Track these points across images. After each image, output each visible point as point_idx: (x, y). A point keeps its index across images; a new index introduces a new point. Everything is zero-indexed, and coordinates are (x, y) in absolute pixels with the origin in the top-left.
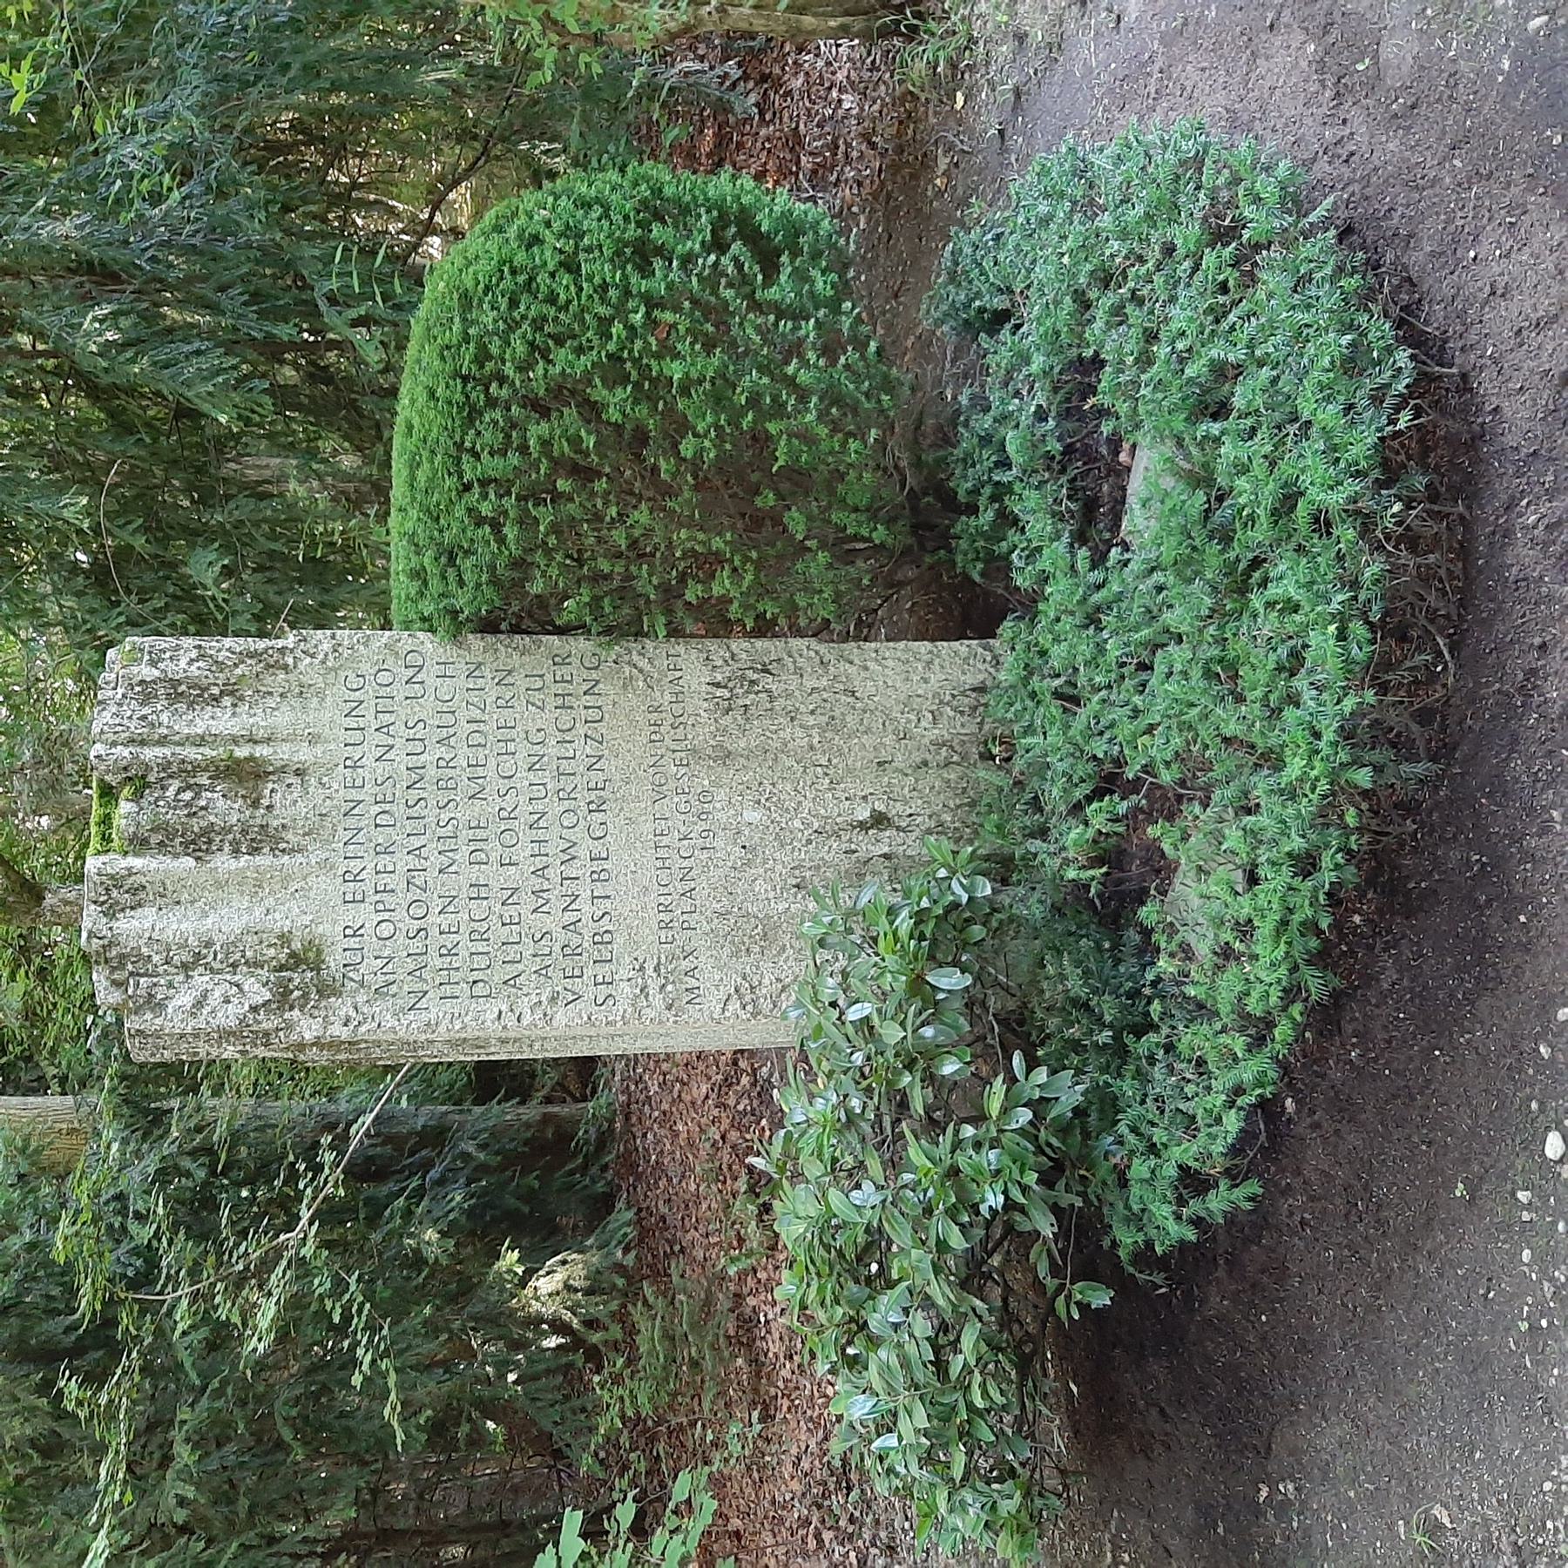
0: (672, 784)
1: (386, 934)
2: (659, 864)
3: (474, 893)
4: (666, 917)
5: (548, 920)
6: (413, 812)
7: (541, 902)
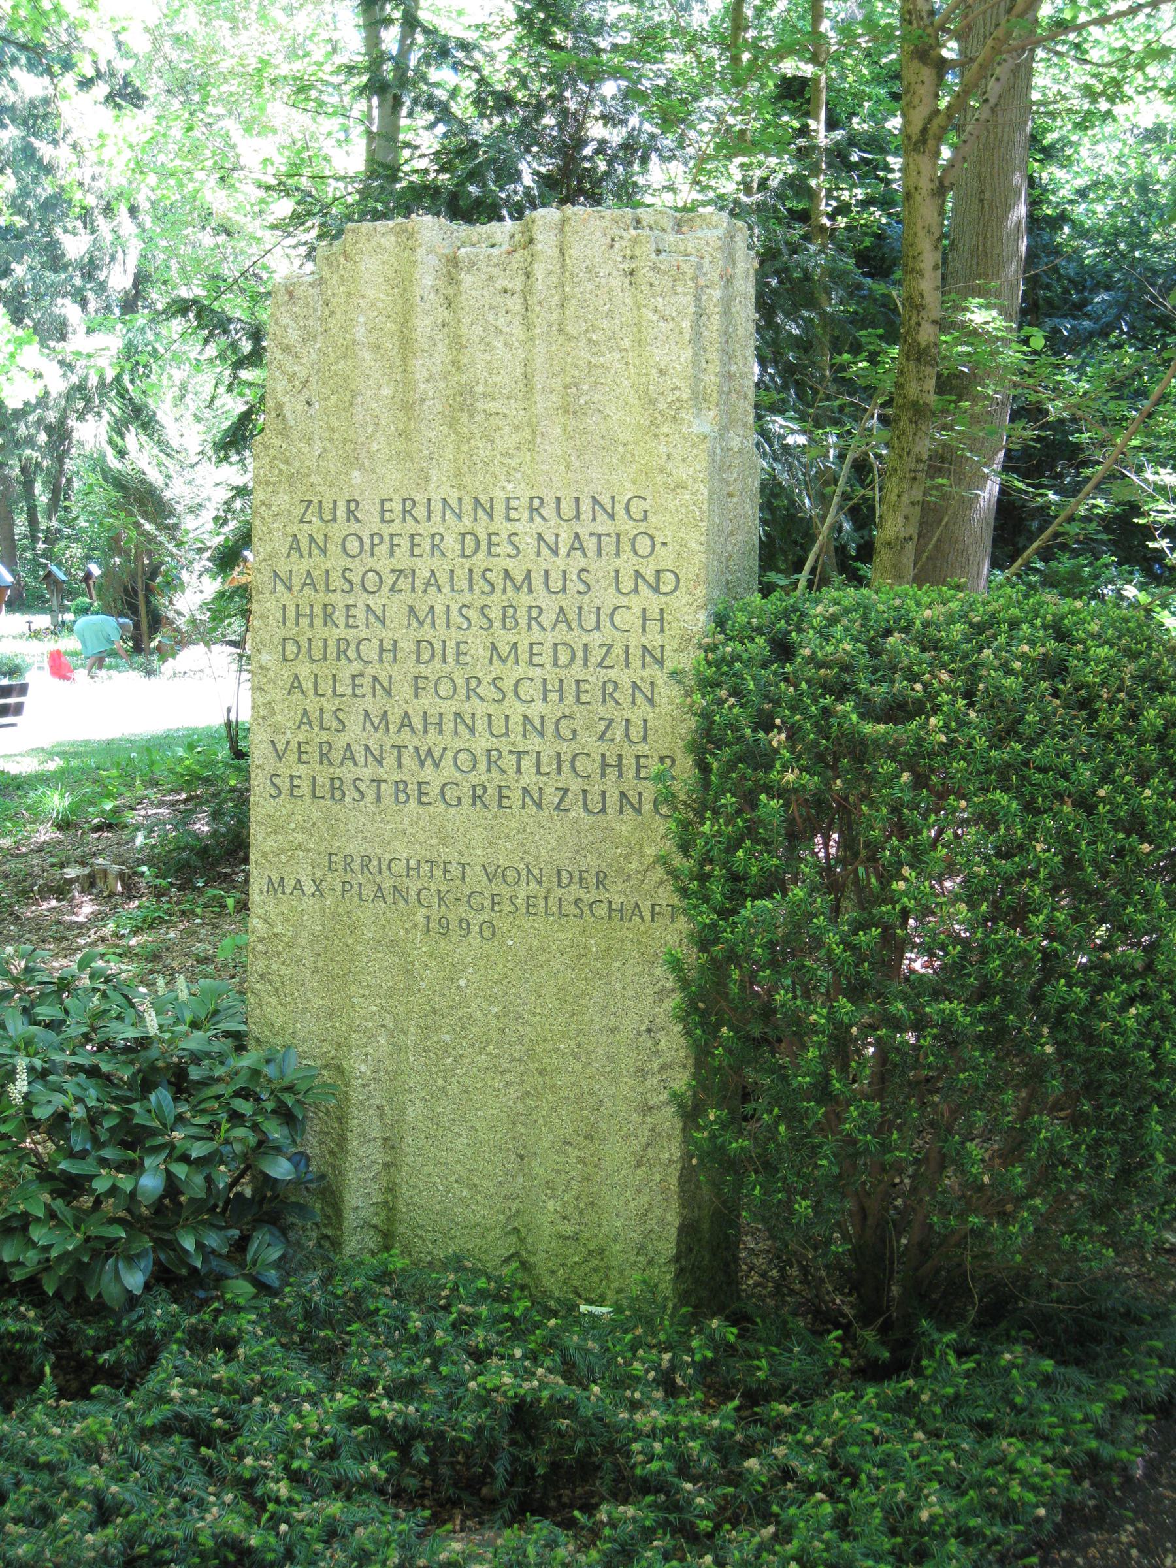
0: (503, 888)
1: (348, 546)
2: (412, 863)
3: (387, 645)
4: (356, 865)
5: (358, 729)
6: (477, 576)
7: (376, 721)
